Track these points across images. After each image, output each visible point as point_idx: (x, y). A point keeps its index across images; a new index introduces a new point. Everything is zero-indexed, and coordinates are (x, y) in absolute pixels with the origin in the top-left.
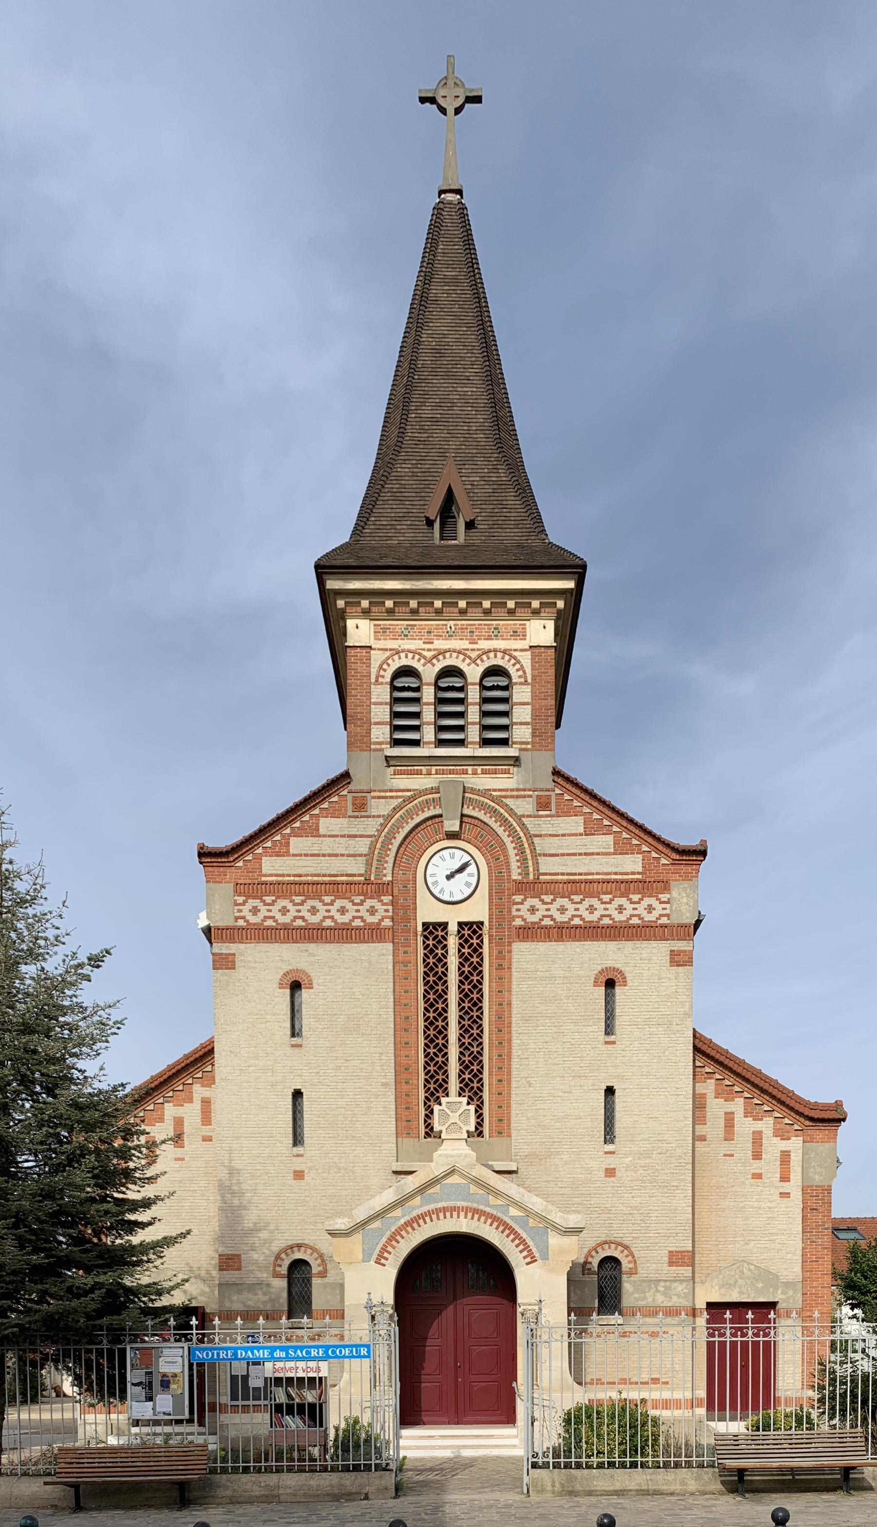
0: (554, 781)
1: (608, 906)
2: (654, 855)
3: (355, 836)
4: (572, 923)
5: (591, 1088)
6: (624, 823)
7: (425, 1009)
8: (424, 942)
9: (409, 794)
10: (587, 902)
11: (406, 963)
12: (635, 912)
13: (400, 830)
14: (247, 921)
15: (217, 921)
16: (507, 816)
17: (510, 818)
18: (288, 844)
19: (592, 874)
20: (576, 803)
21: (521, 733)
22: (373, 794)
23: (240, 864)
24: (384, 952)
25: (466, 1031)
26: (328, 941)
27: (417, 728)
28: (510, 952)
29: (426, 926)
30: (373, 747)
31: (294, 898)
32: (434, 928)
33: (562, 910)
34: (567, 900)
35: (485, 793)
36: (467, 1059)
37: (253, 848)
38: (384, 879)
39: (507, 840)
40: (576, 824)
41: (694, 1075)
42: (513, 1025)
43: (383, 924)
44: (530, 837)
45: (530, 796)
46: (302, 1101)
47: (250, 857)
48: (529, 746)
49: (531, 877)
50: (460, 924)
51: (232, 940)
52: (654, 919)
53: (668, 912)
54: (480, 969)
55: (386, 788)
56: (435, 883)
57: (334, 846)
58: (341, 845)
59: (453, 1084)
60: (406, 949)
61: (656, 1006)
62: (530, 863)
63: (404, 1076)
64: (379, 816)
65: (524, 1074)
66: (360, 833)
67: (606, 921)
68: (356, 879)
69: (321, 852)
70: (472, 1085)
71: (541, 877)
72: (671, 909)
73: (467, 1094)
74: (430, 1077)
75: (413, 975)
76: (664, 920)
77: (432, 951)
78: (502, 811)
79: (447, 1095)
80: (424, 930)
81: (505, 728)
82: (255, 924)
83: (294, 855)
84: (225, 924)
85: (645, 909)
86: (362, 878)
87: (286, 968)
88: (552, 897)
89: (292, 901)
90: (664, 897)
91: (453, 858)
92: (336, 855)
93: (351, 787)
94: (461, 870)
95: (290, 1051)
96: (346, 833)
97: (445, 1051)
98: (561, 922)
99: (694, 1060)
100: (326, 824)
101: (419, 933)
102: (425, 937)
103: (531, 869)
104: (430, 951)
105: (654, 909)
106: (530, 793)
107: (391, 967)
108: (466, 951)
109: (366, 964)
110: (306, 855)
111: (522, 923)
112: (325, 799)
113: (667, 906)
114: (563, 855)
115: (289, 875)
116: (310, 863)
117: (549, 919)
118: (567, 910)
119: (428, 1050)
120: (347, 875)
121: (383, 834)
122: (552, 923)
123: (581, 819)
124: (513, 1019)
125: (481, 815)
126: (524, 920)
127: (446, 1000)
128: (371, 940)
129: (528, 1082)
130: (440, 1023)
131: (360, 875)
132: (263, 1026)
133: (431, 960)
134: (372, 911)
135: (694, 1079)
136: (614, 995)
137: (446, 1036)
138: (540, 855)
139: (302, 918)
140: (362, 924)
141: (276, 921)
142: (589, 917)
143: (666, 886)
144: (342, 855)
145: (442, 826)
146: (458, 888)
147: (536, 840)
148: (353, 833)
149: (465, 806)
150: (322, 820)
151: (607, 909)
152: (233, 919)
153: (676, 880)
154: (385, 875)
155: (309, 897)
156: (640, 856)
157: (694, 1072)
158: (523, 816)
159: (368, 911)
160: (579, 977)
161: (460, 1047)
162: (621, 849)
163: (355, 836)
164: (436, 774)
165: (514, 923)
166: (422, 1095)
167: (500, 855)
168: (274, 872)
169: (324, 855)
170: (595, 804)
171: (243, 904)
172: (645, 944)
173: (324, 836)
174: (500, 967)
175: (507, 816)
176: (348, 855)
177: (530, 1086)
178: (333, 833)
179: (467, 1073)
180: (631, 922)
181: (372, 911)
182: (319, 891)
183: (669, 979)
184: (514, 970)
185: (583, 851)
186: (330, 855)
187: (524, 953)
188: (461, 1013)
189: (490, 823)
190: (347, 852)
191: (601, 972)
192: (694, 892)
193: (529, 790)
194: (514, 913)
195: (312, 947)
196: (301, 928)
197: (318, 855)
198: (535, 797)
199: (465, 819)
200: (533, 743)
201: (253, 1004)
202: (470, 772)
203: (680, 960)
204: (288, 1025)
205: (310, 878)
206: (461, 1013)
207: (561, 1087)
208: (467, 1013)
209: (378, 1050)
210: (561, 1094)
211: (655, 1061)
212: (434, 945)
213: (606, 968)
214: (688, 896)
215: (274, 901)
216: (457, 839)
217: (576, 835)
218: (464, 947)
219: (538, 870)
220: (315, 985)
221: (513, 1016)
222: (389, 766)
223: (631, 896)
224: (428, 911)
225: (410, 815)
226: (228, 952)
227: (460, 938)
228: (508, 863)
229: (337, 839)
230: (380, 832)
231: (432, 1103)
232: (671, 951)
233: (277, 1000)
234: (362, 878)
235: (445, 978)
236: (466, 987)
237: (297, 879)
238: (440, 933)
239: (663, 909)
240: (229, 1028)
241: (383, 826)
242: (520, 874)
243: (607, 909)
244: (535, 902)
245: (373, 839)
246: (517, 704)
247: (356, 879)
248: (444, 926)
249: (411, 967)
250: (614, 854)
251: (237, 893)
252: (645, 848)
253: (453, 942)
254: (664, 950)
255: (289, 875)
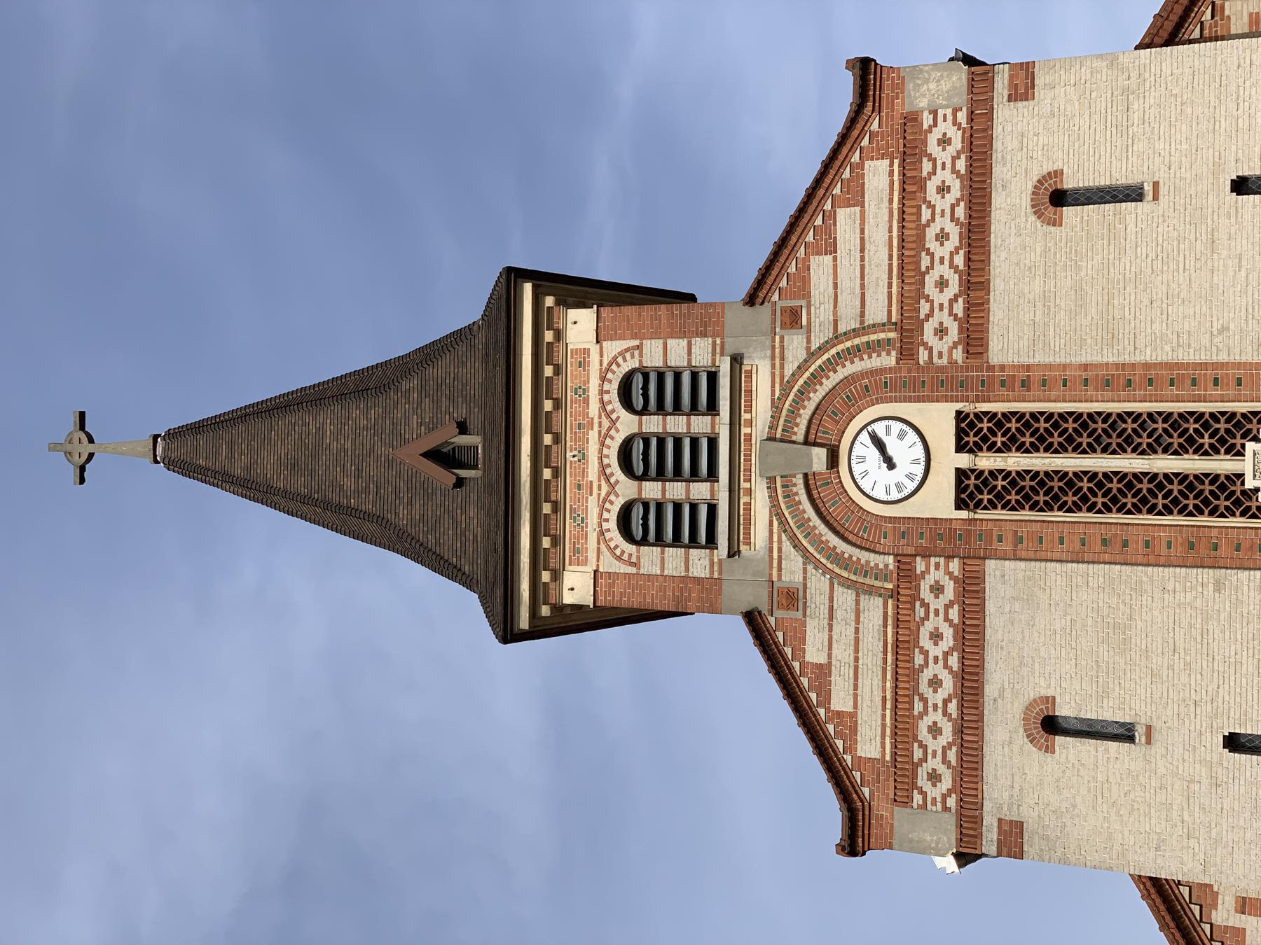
0: (762, 303)
1: (938, 211)
2: (865, 142)
3: (831, 608)
4: (961, 267)
5: (1233, 220)
6: (821, 192)
7: (1089, 510)
8: (985, 508)
9: (775, 523)
10: (932, 244)
11: (1018, 540)
12: (949, 165)
13: (824, 539)
14: (950, 791)
15: (949, 839)
16: (807, 374)
17: (811, 370)
18: (840, 714)
19: (891, 238)
20: (792, 269)
21: (702, 353)
22: (775, 579)
23: (866, 791)
24: (998, 573)
25: (1128, 441)
26: (981, 666)
27: (694, 508)
28: (1002, 367)
29: (960, 504)
30: (716, 575)
31: (916, 713)
32: (964, 490)
33: (942, 284)
34: (927, 277)
35: (776, 406)
36: (1176, 441)
37: (844, 769)
38: (891, 567)
39: (842, 373)
40: (820, 267)
41: (1217, 39)
42: (1121, 360)
43: (956, 573)
44: (837, 338)
45: (782, 338)
46: (1245, 735)
47: (857, 776)
48: (718, 341)
49: (892, 335)
50: (960, 448)
51: (977, 821)
52: (960, 133)
53: (949, 112)
54: (1028, 416)
55: (767, 558)
56: (899, 487)
57: (845, 642)
58: (844, 631)
59: (1222, 465)
60: (995, 538)
61: (1097, 117)
62: (874, 337)
63: (1204, 552)
64: (805, 571)
65: (1205, 340)
66: (827, 601)
67: (960, 212)
68: (890, 613)
69: (852, 664)
70: (1222, 432)
71: (894, 320)
72: (946, 107)
73: (1238, 441)
74: (1206, 506)
75: (1035, 527)
76: (962, 117)
77: (999, 496)
78: (801, 382)
79: (1240, 476)
80: (967, 507)
81: (695, 376)
82: (954, 780)
83: (855, 706)
84: (954, 828)
85: (944, 150)
86: (890, 601)
87: (1021, 738)
88: (922, 301)
89: (921, 716)
90: (927, 120)
91: (864, 458)
92: (857, 640)
93: (765, 612)
94: (880, 445)
95: (1157, 748)
96: (826, 622)
97: (1161, 477)
98: (960, 286)
99: (1190, 42)
100: (814, 653)
101: (972, 515)
102: (977, 505)
103: (882, 336)
104: (1000, 500)
105: (945, 134)
106: (777, 338)
107: (1022, 564)
108: (999, 440)
109: (1017, 606)
110: (856, 687)
111: (960, 348)
112: (779, 651)
113: (941, 113)
114: (863, 286)
115: (884, 716)
116: (867, 683)
117: (955, 305)
118: (942, 277)
119: (1160, 507)
120: (885, 626)
121: (829, 565)
122: (960, 300)
123: (815, 261)
124: (1111, 360)
125: (806, 414)
126: (955, 345)
127: (1075, 474)
128: (980, 594)
129: (1220, 332)
130: (1114, 486)
131: (885, 605)
132: (1114, 788)
133: (1013, 497)
134: (937, 589)
135: (1223, 38)
136: (1076, 191)
137: (1135, 475)
138: (862, 322)
139: (946, 702)
140: (956, 607)
141: (950, 745)
142: (954, 240)
143: (912, 119)
144: (857, 630)
145: (820, 473)
146: (906, 450)
147: (842, 328)
148: (827, 611)
149: (794, 438)
150: (809, 658)
151: (943, 211)
152: (947, 815)
153: (903, 104)
154: (887, 566)
155: (916, 689)
156: (867, 163)
157: (1211, 39)
158: (808, 348)
159: (937, 597)
160: (1046, 251)
161: (1155, 452)
162: (856, 196)
163: (831, 608)
164: (750, 481)
165: (960, 362)
166: (1238, 521)
167: (861, 385)
168: (878, 738)
169: (856, 659)
170: (794, 239)
171: (924, 794)
172: (997, 145)
173: (830, 656)
174: (1026, 384)
175: (807, 374)
176: (858, 621)
177: (1228, 329)
178: (826, 643)
179: (1201, 441)
180: (963, 172)
181: (937, 589)
182: (907, 672)
183: (1054, 99)
184: (1031, 361)
185: (858, 255)
186: (856, 650)
187: (1006, 346)
188: (1099, 449)
189: (818, 400)
190: (853, 623)
191: (1039, 214)
192: (921, 71)
193: (774, 341)
194: (945, 361)
195: (990, 690)
196: (961, 706)
197: (856, 668)
198: (784, 332)
199: (812, 437)
200: (714, 336)
201: (1079, 799)
202: (748, 430)
203: (1024, 83)
204: (1113, 745)
205: (888, 684)
206: (1099, 449)
207: (1231, 273)
208: (1098, 440)
209: (1158, 595)
210: (1243, 273)
211: (1189, 111)
212: (989, 493)
213: (1033, 206)
214: (927, 81)
215: (921, 745)
216: (838, 451)
217: (835, 267)
218: (994, 443)
219: (884, 325)
220: (1050, 693)
221: (1105, 360)
222: (739, 552)
223: (925, 174)
224: (938, 500)
225: (803, 523)
226: (996, 830)
227: (981, 449)
228: (873, 372)
229: (835, 637)
230: (826, 571)
231: (1254, 505)
232: (1010, 100)
233: (1072, 759)
234: (890, 601)
235: (1042, 475)
236: (1056, 439)
237: (889, 705)
238: (972, 481)
239: (945, 120)
240: (1117, 847)
241: (818, 565)
242: (889, 354)
243: (943, 211)
244: (929, 328)
245: (836, 582)
246: (665, 361)
247: (890, 613)
248: (961, 474)
249: (1023, 531)
250: (863, 206)
251: (907, 802)
252: (856, 158)
253: (987, 461)
254: (1007, 112)
255: (884, 716)
